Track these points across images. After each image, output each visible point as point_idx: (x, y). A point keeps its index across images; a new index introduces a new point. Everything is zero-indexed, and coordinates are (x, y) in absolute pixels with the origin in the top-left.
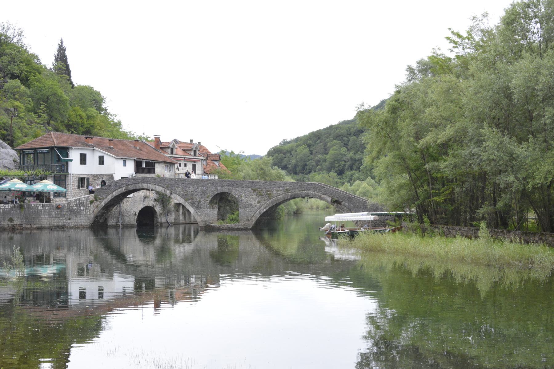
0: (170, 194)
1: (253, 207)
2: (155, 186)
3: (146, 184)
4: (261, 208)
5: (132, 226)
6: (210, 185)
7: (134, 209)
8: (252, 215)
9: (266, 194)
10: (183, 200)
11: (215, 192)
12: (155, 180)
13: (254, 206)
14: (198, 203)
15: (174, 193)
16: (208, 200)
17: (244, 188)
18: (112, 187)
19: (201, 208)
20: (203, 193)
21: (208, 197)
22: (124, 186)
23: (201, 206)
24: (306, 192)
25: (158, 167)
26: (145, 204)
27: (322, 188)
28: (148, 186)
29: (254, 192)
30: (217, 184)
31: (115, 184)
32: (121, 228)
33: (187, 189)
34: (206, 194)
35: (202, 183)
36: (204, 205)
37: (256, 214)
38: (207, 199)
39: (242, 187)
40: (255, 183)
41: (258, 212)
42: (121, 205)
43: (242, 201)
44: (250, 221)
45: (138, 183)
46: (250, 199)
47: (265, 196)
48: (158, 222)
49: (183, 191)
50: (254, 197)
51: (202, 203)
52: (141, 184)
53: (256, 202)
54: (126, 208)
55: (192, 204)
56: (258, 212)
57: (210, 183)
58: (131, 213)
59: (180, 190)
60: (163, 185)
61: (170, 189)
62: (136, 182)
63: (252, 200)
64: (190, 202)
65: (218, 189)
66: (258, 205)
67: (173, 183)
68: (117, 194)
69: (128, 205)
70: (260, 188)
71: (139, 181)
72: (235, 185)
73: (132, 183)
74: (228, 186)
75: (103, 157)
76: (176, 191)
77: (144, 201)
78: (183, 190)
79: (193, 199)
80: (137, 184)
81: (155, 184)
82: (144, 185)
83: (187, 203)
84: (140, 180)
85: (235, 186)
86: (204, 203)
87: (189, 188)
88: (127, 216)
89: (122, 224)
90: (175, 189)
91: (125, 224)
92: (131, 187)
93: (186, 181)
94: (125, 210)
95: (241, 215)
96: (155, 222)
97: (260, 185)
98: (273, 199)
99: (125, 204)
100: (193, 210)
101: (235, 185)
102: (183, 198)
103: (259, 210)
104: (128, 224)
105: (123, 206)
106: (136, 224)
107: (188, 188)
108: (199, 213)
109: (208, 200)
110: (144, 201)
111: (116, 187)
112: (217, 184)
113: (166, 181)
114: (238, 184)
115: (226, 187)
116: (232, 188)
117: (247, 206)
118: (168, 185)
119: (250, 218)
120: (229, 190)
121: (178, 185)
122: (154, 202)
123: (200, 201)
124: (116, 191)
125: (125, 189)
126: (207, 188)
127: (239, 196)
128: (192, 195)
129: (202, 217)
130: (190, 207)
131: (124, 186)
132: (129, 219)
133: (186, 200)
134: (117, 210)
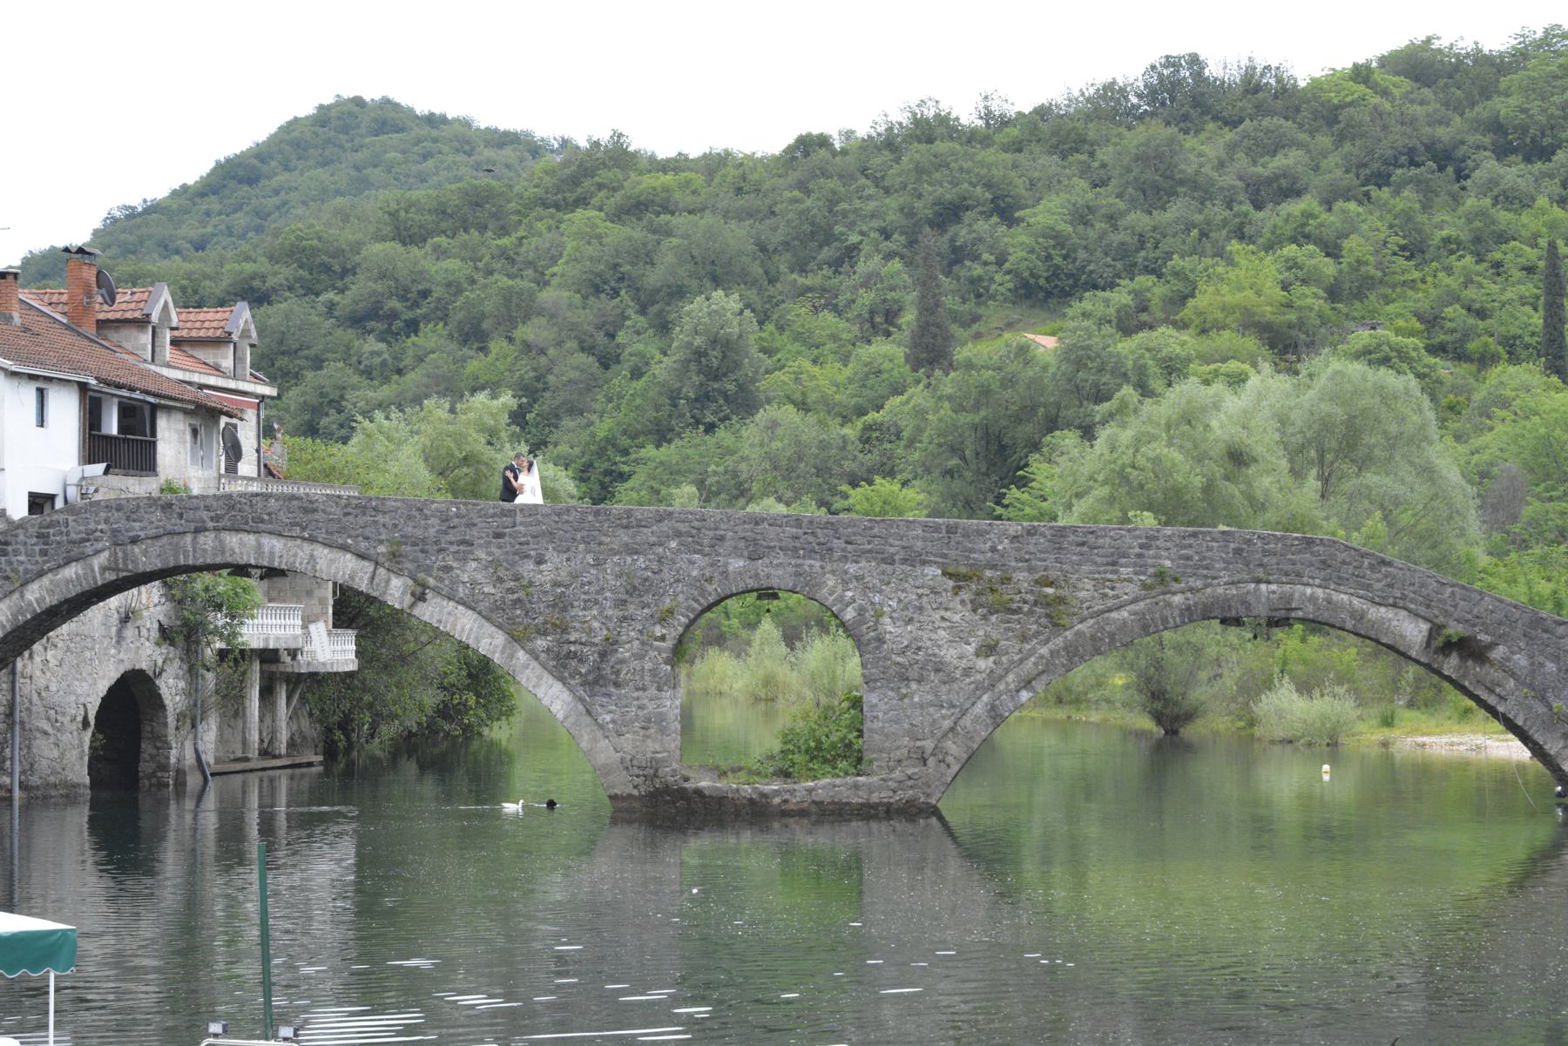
0: (408, 599)
1: (954, 680)
2: (307, 547)
3: (250, 539)
4: (1002, 686)
5: (69, 795)
6: (673, 544)
7: (81, 688)
8: (947, 724)
9: (1036, 603)
10: (500, 638)
11: (710, 588)
12: (306, 511)
13: (958, 674)
14: (603, 655)
15: (435, 590)
16: (663, 638)
17: (892, 563)
18: (16, 553)
19: (617, 685)
20: (632, 590)
21: (662, 621)
22: (99, 545)
23: (618, 673)
24: (1273, 587)
25: (167, 434)
26: (122, 656)
27: (1372, 567)
28: (259, 546)
29: (957, 590)
30: (722, 539)
31: (42, 537)
32: (16, 804)
33: (527, 568)
34: (648, 598)
35: (620, 532)
36: (635, 664)
37: (967, 721)
38: (658, 631)
39: (884, 561)
40: (966, 536)
41: (979, 709)
42: (19, 664)
43: (880, 640)
44: (931, 762)
45: (197, 531)
46: (935, 630)
47: (1031, 612)
48: (164, 767)
49: (500, 580)
50: (957, 618)
51: (623, 652)
52: (212, 535)
53: (971, 649)
54: (41, 681)
55: (561, 664)
56: (979, 709)
57: (678, 534)
58: (64, 714)
59: (479, 577)
60: (363, 545)
61: (409, 565)
62: (180, 525)
63: (942, 633)
64: (548, 651)
65: (731, 568)
66: (983, 664)
67: (432, 531)
68: (50, 601)
69: (53, 662)
70: (993, 567)
71: (205, 515)
72: (838, 544)
73: (152, 532)
74: (796, 549)
76: (455, 582)
77: (120, 637)
78: (501, 573)
79: (565, 631)
80: (189, 538)
81: (312, 540)
82: (233, 540)
83: (521, 655)
84: (207, 509)
85: (837, 555)
86: (640, 657)
87: (540, 561)
88: (46, 733)
89: (21, 783)
90: (447, 569)
91: (35, 780)
92: (145, 553)
93: (519, 518)
94: (35, 698)
95: (877, 725)
96: (145, 767)
97: (993, 550)
98: (1079, 634)
99: (38, 659)
100: (566, 696)
101: (838, 544)
102: (499, 627)
103: (985, 698)
104: (52, 779)
105: (28, 671)
106: (87, 780)
107: (530, 565)
108: (608, 718)
109: (663, 638)
110: (120, 637)
111: (44, 553)
112: (722, 539)
113: (380, 518)
114: (859, 539)
115: (782, 558)
116: (818, 564)
117: (913, 673)
118: (399, 544)
119: (929, 745)
120: (798, 574)
121: (462, 542)
122: (158, 644)
123: (611, 643)
124: (46, 580)
125: (104, 569)
126: (655, 566)
127: (861, 611)
128: (562, 604)
129: (628, 742)
130: (548, 679)
131: (99, 545)
132: (56, 753)
133: (517, 637)
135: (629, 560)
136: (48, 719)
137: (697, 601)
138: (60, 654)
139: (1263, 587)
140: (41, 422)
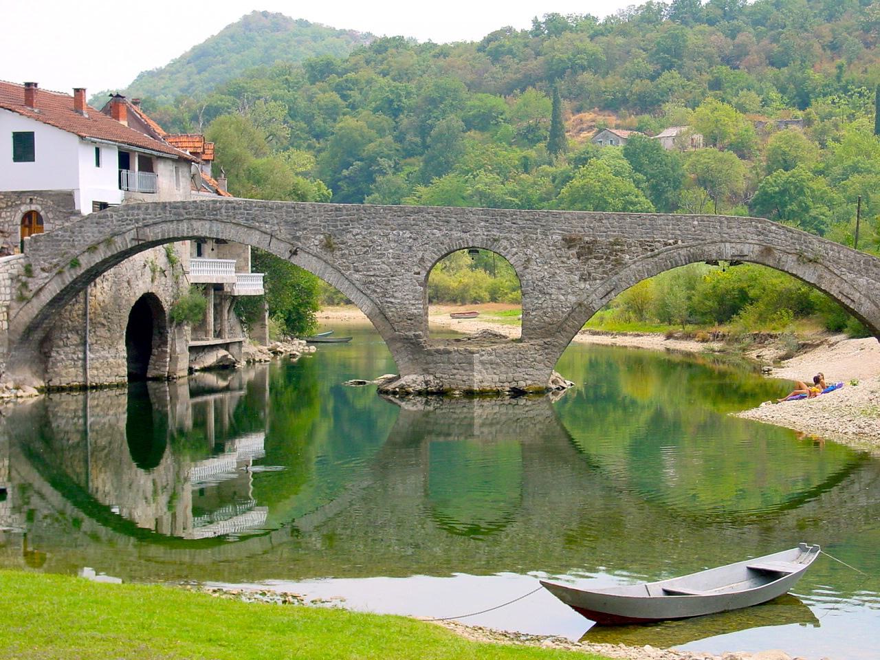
0: (287, 255)
3: (207, 225)
16: (419, 273)
42: (89, 291)
69: (106, 288)
75: (30, 136)
93: (345, 212)
99: (98, 287)
134: (76, 308)
135: (401, 233)
136: (105, 317)
137: (436, 254)
138: (110, 284)
139: (728, 245)
140: (98, 164)
